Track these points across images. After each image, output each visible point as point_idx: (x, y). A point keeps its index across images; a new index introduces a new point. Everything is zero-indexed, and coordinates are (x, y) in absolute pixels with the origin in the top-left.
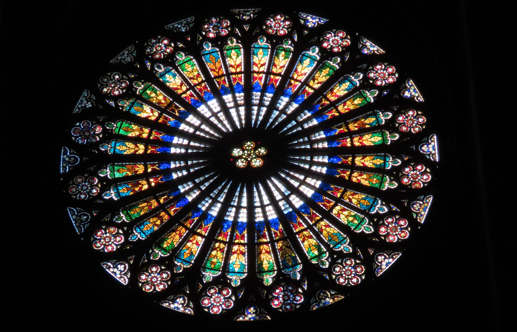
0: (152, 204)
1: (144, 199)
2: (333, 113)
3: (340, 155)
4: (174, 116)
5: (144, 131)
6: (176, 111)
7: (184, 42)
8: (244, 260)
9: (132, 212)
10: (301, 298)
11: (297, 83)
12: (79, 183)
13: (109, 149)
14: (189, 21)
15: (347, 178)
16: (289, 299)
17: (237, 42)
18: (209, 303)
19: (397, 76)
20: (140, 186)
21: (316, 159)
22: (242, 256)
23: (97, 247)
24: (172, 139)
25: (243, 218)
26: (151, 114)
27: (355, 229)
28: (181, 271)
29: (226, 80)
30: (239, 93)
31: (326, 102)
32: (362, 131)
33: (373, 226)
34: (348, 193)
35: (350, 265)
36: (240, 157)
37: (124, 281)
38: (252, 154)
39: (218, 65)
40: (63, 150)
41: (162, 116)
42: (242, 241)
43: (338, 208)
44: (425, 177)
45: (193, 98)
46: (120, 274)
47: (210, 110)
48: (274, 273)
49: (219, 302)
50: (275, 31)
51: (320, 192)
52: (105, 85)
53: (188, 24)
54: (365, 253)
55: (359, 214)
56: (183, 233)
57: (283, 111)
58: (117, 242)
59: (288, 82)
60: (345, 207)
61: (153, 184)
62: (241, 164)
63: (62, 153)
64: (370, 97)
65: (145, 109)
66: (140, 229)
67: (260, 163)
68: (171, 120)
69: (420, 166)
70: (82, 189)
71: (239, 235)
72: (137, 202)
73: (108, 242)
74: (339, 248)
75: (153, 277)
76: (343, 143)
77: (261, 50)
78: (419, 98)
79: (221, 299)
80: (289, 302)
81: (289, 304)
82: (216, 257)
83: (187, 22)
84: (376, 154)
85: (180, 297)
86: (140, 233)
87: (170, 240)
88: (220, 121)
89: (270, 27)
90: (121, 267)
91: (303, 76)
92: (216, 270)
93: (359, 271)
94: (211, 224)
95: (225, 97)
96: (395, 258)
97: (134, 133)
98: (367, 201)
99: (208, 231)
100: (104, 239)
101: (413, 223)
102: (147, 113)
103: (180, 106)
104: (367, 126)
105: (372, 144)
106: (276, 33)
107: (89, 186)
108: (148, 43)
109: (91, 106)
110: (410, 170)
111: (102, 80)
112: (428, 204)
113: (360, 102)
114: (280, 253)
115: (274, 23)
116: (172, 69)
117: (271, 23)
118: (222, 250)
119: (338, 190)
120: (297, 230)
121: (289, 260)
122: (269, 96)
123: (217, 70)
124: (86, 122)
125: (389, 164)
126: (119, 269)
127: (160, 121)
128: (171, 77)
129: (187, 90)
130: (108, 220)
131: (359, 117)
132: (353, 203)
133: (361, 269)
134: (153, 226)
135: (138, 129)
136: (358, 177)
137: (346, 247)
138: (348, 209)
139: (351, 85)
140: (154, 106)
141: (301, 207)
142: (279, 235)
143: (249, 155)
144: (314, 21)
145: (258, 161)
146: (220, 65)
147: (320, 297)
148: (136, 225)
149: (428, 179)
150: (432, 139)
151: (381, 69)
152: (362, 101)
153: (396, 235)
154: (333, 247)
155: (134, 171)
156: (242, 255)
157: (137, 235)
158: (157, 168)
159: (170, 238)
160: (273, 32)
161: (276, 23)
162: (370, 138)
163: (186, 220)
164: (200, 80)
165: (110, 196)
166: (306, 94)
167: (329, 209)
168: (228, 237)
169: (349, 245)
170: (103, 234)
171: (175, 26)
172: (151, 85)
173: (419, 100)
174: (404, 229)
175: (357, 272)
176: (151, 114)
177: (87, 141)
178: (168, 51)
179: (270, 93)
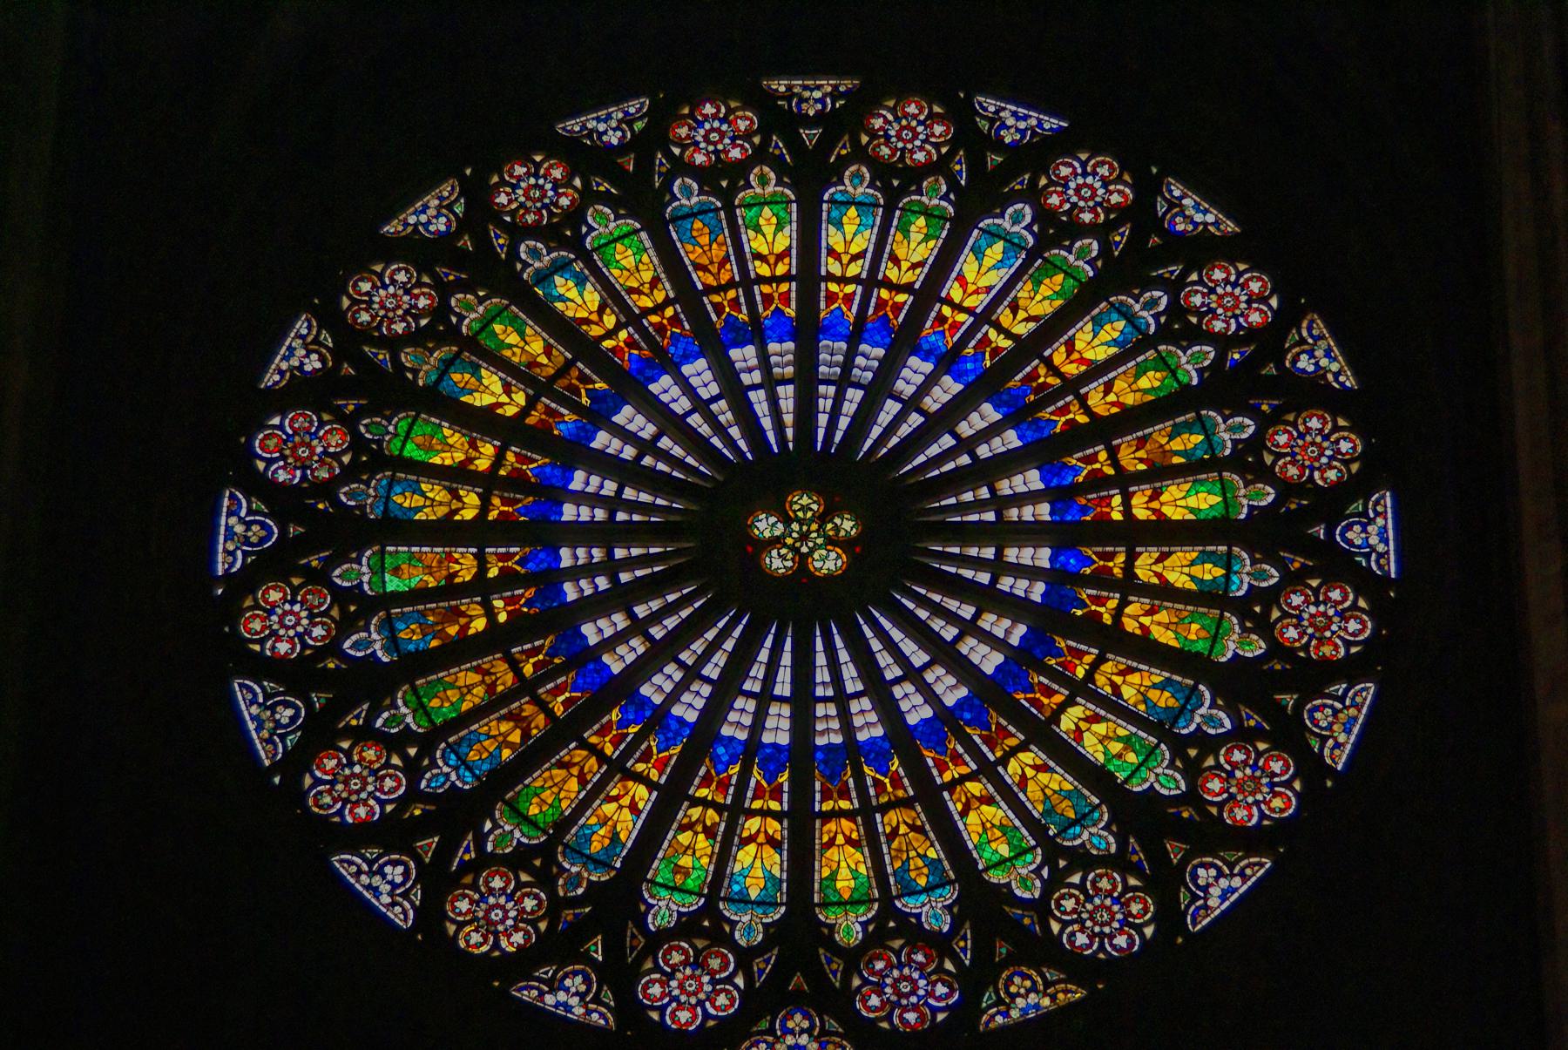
0: (497, 679)
1: (475, 663)
2: (1071, 416)
3: (1089, 546)
4: (576, 407)
5: (482, 450)
6: (583, 391)
8: (775, 862)
9: (435, 703)
11: (961, 317)
12: (274, 605)
13: (369, 501)
14: (632, 110)
15: (1107, 619)
16: (913, 992)
17: (779, 183)
18: (663, 995)
19: (1274, 302)
20: (463, 621)
21: (1011, 554)
22: (772, 851)
23: (321, 807)
25: (778, 730)
26: (504, 399)
27: (1126, 781)
28: (580, 891)
29: (742, 300)
30: (781, 341)
31: (1050, 380)
32: (1160, 473)
33: (1184, 773)
34: (1108, 667)
36: (777, 541)
37: (401, 916)
39: (717, 252)
40: (226, 500)
41: (540, 407)
42: (774, 805)
43: (1075, 712)
44: (1353, 626)
45: (636, 352)
46: (391, 894)
47: (689, 390)
48: (870, 909)
49: (695, 994)
51: (1022, 660)
52: (364, 302)
53: (629, 120)
55: (1141, 733)
56: (590, 771)
57: (911, 404)
58: (385, 794)
59: (933, 314)
60: (1098, 710)
61: (502, 617)
62: (777, 562)
63: (225, 510)
64: (1189, 367)
65: (485, 382)
66: (457, 755)
67: (839, 563)
68: (566, 419)
69: (1338, 591)
70: (282, 625)
71: (765, 785)
72: (452, 671)
73: (358, 792)
74: (1075, 839)
76: (1099, 509)
77: (852, 212)
78: (1342, 379)
79: (701, 985)
80: (914, 999)
81: (915, 1008)
82: (690, 852)
83: (626, 113)
85: (575, 973)
86: (456, 769)
87: (549, 792)
88: (720, 430)
89: (882, 140)
90: (396, 873)
91: (982, 297)
92: (691, 893)
93: (1134, 912)
94: (679, 749)
95: (735, 354)
96: (1250, 877)
97: (449, 454)
98: (1167, 694)
99: (669, 769)
100: (346, 782)
101: (1310, 766)
102: (493, 394)
103: (595, 377)
104: (1177, 460)
105: (1191, 517)
107: (304, 614)
108: (501, 178)
109: (318, 365)
110: (1307, 602)
111: (355, 285)
112: (1359, 711)
113: (1157, 384)
114: (889, 847)
116: (575, 260)
118: (710, 832)
119: (1080, 655)
120: (947, 777)
121: (918, 868)
123: (715, 270)
124: (301, 415)
125: (1242, 582)
126: (389, 878)
127: (531, 420)
128: (571, 284)
129: (619, 326)
130: (361, 722)
131: (1151, 430)
132: (1125, 697)
133: (1141, 906)
134: (499, 748)
135: (462, 444)
136: (1142, 619)
137: (1098, 837)
138: (1109, 716)
139: (1129, 329)
140: (516, 374)
141: (960, 703)
143: (804, 537)
144: (1022, 125)
146: (723, 254)
147: (1013, 989)
148: (447, 743)
149: (1361, 631)
151: (1227, 281)
152: (1162, 381)
153: (1257, 803)
154: (1055, 835)
155: (444, 573)
156: (774, 847)
157: (447, 775)
158: (518, 568)
159: (550, 787)
160: (893, 155)
161: (903, 128)
162: (1184, 498)
163: (602, 732)
164: (660, 296)
165: (368, 648)
166: (987, 354)
167: (1048, 714)
168: (731, 790)
170: (344, 767)
171: (589, 126)
172: (507, 307)
173: (1342, 384)
174: (1280, 784)
175: (1130, 914)
176: (504, 399)
177: (304, 478)
178: (564, 201)
179: (875, 345)
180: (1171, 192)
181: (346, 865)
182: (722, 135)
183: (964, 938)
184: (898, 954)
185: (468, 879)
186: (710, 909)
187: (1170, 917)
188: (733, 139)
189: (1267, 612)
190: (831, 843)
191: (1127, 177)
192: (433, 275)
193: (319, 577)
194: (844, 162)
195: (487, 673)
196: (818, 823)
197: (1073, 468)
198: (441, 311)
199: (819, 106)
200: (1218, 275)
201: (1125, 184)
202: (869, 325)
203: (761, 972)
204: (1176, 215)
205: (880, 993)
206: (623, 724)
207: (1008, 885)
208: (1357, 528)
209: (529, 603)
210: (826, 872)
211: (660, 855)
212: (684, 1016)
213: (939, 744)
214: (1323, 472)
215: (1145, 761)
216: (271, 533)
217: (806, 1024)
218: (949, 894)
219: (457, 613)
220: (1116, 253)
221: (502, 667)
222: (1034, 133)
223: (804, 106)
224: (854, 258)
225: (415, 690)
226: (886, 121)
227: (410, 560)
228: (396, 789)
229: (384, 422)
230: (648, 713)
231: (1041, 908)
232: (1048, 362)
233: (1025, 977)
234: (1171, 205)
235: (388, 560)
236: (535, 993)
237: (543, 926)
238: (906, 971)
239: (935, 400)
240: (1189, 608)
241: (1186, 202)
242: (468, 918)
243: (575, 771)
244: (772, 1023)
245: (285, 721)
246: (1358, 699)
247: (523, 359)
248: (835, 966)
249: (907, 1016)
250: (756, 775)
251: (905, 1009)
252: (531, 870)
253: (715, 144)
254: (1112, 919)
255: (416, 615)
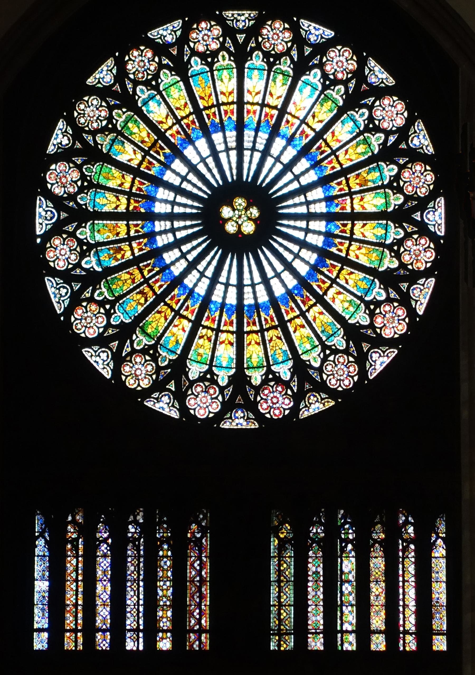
3: (339, 221)
4: (159, 161)
7: (170, 56)
9: (114, 287)
10: (291, 402)
13: (88, 201)
14: (175, 25)
17: (230, 60)
20: (122, 252)
23: (77, 329)
24: (156, 192)
25: (232, 299)
27: (349, 319)
30: (231, 131)
33: (369, 315)
34: (344, 272)
35: (343, 364)
36: (230, 219)
37: (107, 374)
38: (243, 216)
39: (208, 91)
41: (146, 160)
42: (231, 329)
44: (428, 254)
45: (179, 136)
46: (103, 364)
49: (205, 403)
50: (272, 46)
51: (315, 268)
54: (359, 348)
55: (355, 299)
62: (231, 228)
66: (122, 307)
70: (61, 255)
73: (90, 323)
75: (137, 369)
78: (428, 148)
79: (207, 400)
80: (278, 405)
83: (174, 27)
84: (377, 222)
85: (165, 395)
86: (123, 314)
87: (154, 323)
88: (210, 170)
89: (266, 40)
90: (104, 356)
92: (203, 363)
94: (198, 305)
98: (364, 283)
101: (411, 312)
103: (165, 147)
104: (371, 185)
106: (273, 49)
107: (68, 249)
108: (129, 57)
109: (67, 142)
111: (79, 106)
113: (364, 151)
115: (272, 33)
117: (268, 33)
118: (209, 339)
122: (263, 136)
123: (207, 99)
126: (102, 358)
129: (174, 124)
134: (137, 305)
139: (355, 126)
141: (295, 288)
142: (270, 322)
143: (240, 217)
144: (317, 33)
145: (250, 224)
147: (310, 401)
150: (440, 205)
153: (393, 327)
154: (326, 340)
155: (115, 232)
157: (120, 316)
158: (141, 230)
160: (270, 47)
161: (274, 34)
163: (172, 299)
166: (304, 137)
169: (343, 338)
172: (133, 115)
173: (428, 151)
175: (349, 372)
177: (65, 191)
178: (152, 68)
180: (370, 64)
181: (87, 353)
182: (209, 36)
183: (294, 381)
184: (272, 387)
185: (128, 358)
186: (210, 371)
187: (363, 373)
188: (213, 39)
189: (399, 249)
190: (250, 344)
191: (355, 58)
192: (107, 102)
193: (72, 235)
194: (253, 50)
195: (131, 274)
196: (246, 335)
197: (333, 187)
198: (110, 119)
199: (243, 24)
200: (386, 102)
201: (354, 60)
202: (262, 124)
203: (227, 394)
204: (372, 74)
205: (267, 403)
206: (179, 295)
207: (309, 361)
208: (431, 213)
209: (145, 245)
210: (248, 356)
211: (193, 348)
212: (202, 412)
213: (287, 304)
214: (420, 189)
215: (356, 310)
216: (54, 216)
217: (242, 415)
218: (290, 363)
219: (120, 249)
220: (350, 92)
221: (137, 272)
222: (322, 38)
223: (238, 23)
224: (257, 93)
225: (107, 281)
226: (269, 31)
227: (103, 226)
228: (102, 322)
229: (92, 167)
230: (188, 291)
231: (320, 370)
232: (325, 141)
233: (315, 396)
234: (371, 70)
235: (96, 227)
236: (152, 403)
237: (154, 377)
238: (275, 394)
239: (286, 159)
240: (373, 247)
241: (376, 69)
242: (129, 374)
243: (163, 314)
244: (231, 414)
245: (63, 294)
246: (429, 285)
247: (140, 139)
248: (251, 392)
249: (275, 411)
250: (225, 317)
251: (275, 409)
252: (150, 355)
253: (206, 41)
254: (344, 373)
255: (106, 250)
